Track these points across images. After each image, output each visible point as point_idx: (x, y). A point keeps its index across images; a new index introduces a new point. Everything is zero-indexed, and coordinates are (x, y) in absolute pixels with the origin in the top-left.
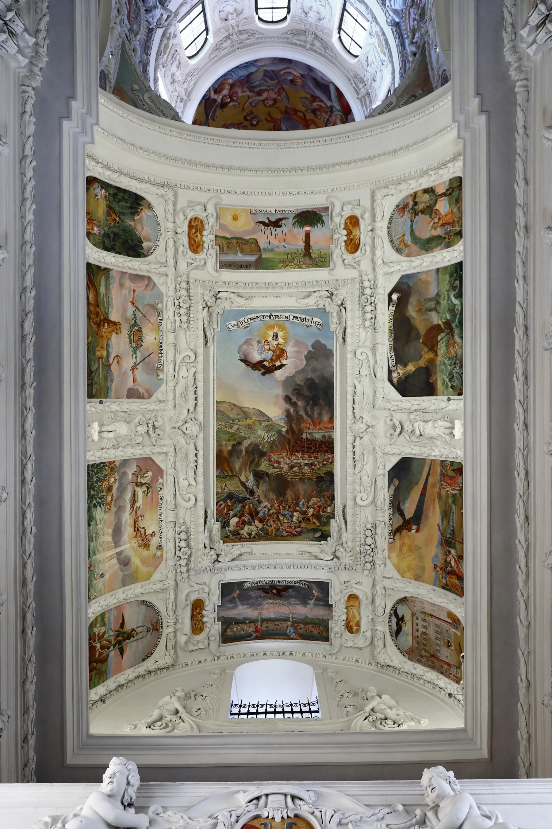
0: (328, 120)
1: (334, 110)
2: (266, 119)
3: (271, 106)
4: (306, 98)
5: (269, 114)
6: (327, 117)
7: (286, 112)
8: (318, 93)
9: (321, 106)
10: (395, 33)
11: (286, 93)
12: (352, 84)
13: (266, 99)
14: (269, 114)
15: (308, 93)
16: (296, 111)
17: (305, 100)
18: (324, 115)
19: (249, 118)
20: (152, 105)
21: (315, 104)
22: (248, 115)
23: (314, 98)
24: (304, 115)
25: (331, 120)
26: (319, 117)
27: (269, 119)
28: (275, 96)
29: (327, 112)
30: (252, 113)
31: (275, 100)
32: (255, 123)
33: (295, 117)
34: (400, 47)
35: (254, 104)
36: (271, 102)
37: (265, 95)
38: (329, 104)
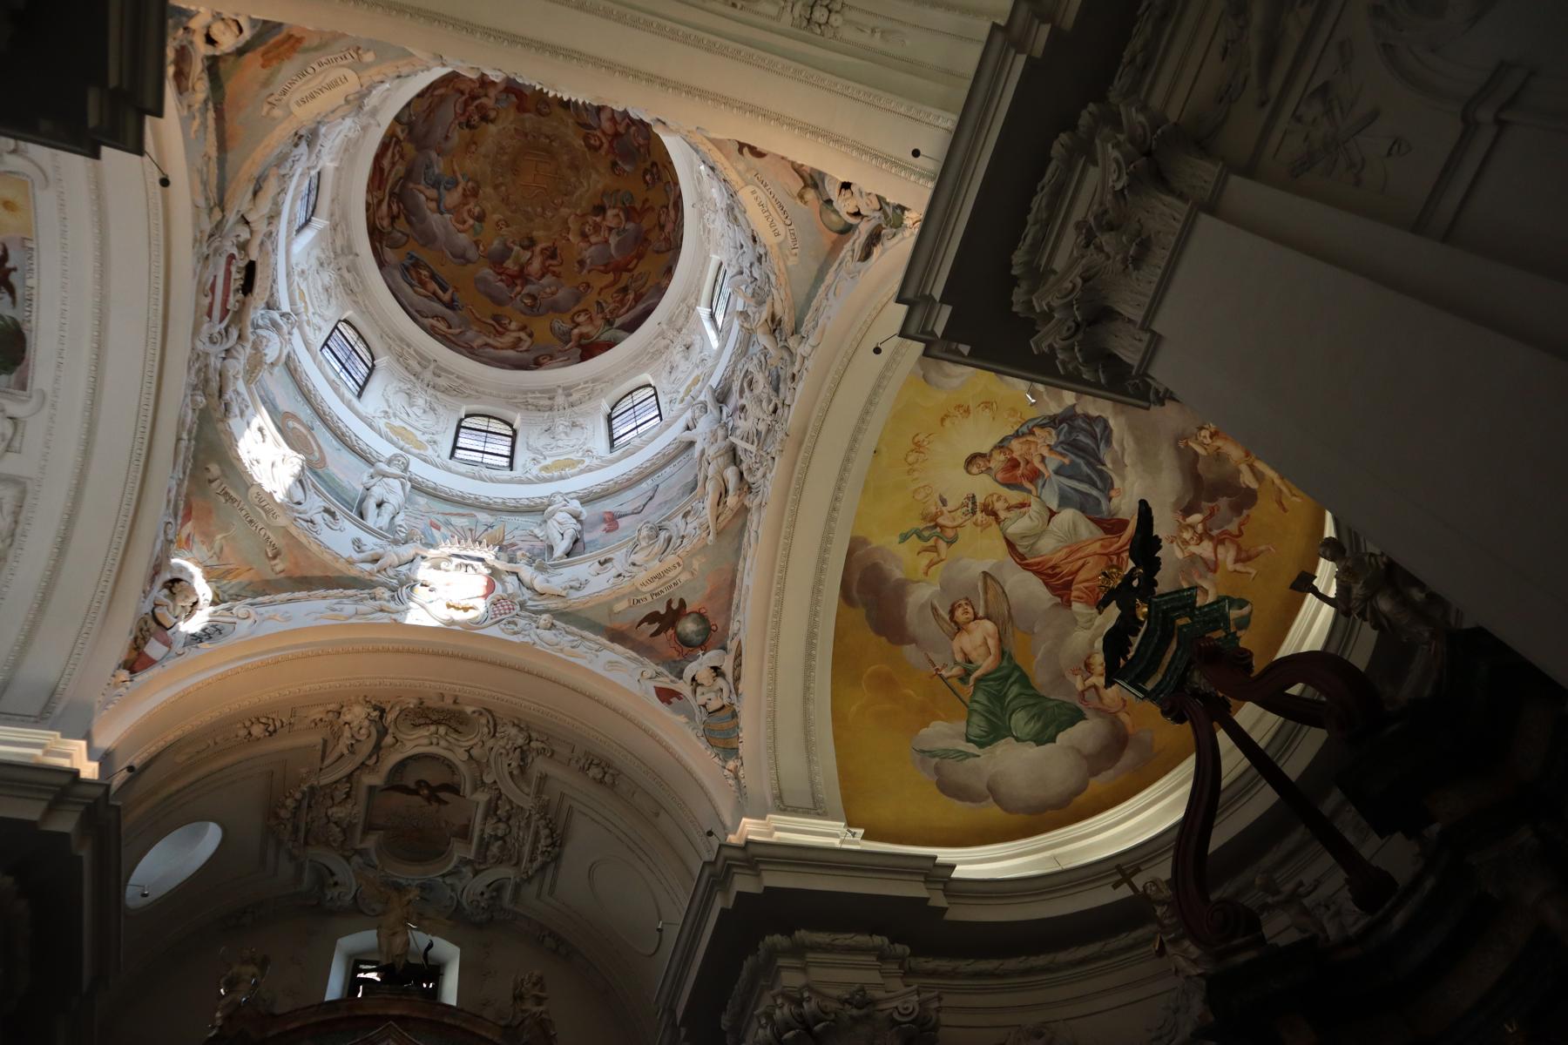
0: (603, 311)
1: (606, 328)
2: (647, 200)
3: (659, 216)
4: (644, 286)
5: (651, 209)
6: (607, 311)
7: (646, 240)
8: (640, 307)
9: (625, 305)
10: (538, 501)
11: (663, 252)
12: (586, 382)
13: (668, 214)
14: (651, 209)
15: (648, 290)
16: (640, 257)
17: (640, 283)
18: (611, 307)
19: (655, 170)
20: (327, 81)
21: (631, 296)
22: (658, 171)
23: (638, 299)
24: (630, 271)
25: (600, 316)
26: (615, 295)
27: (646, 206)
28: (667, 230)
29: (611, 313)
30: (659, 178)
31: (662, 227)
32: (648, 177)
33: (633, 253)
34: (512, 503)
35: (668, 189)
36: (663, 218)
37: (672, 213)
38: (618, 322)
